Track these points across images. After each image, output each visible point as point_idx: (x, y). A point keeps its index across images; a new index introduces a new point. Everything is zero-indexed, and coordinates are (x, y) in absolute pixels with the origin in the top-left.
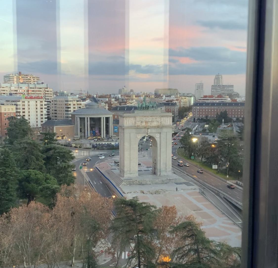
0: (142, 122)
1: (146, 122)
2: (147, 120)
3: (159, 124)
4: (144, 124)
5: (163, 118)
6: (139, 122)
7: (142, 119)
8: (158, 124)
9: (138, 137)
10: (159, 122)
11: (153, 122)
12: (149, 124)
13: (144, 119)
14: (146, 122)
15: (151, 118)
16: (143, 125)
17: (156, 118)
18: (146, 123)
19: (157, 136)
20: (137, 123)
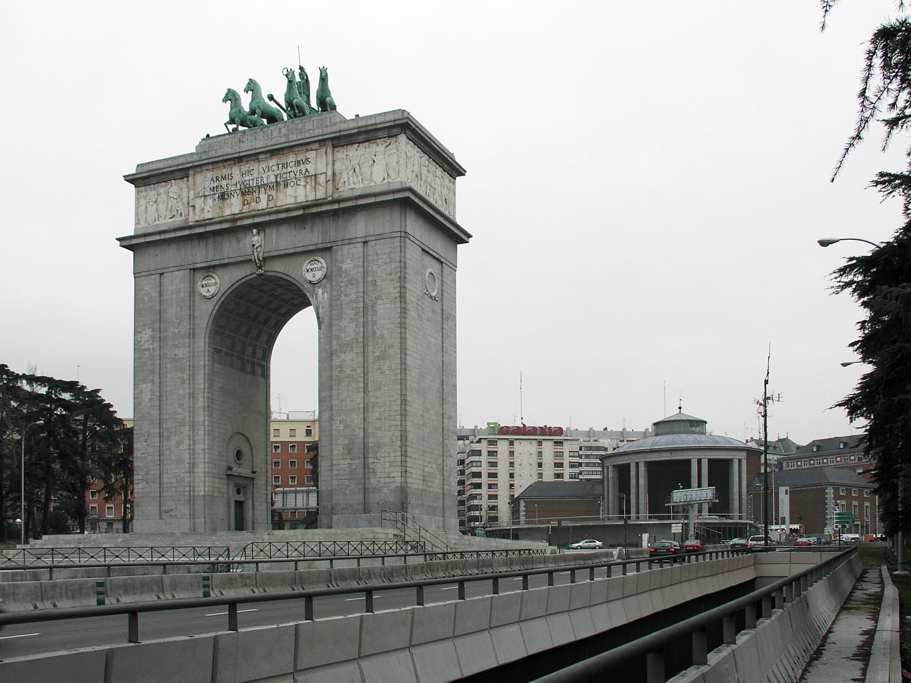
0: (223, 197)
1: (246, 191)
2: (251, 180)
3: (321, 194)
4: (234, 206)
5: (341, 154)
6: (210, 201)
7: (224, 178)
8: (311, 197)
9: (203, 291)
10: (322, 179)
11: (286, 185)
12: (263, 204)
13: (237, 178)
14: (246, 191)
15: (273, 162)
16: (227, 212)
17: (300, 158)
18: (248, 197)
19: (309, 276)
20: (199, 203)
